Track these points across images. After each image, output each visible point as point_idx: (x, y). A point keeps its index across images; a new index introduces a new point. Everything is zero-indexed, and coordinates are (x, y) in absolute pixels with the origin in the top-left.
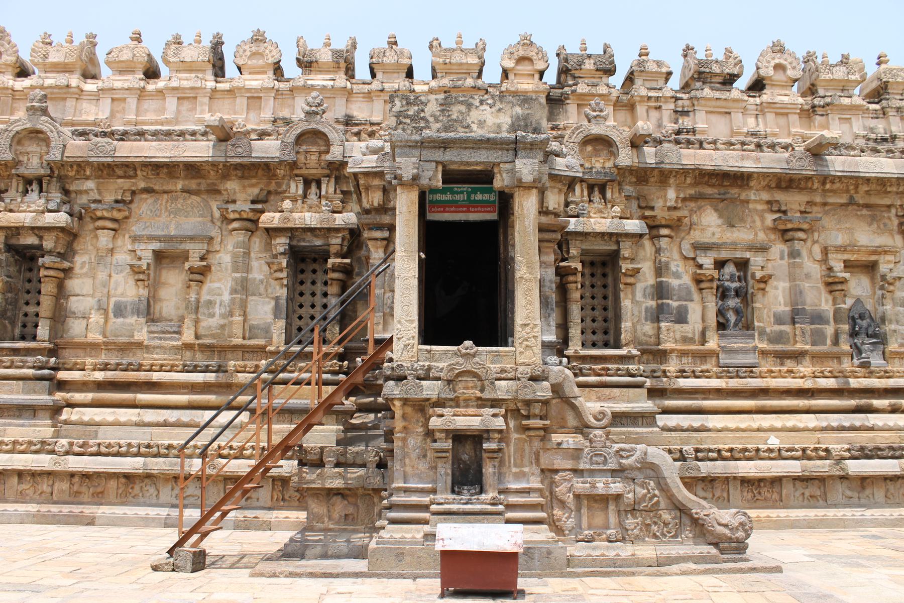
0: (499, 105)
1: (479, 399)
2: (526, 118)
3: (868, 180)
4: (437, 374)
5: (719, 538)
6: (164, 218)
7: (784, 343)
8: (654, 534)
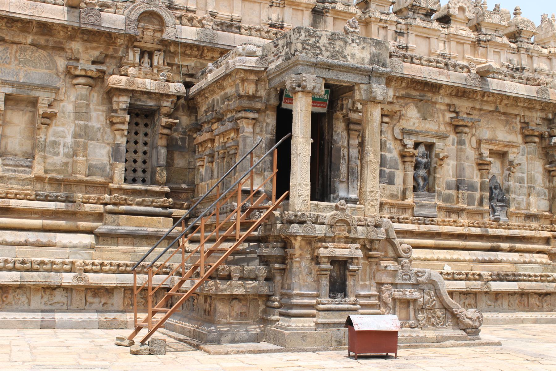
0: (362, 45)
1: (346, 237)
2: (378, 55)
3: (508, 97)
4: (322, 221)
5: (466, 326)
6: (13, 66)
7: (451, 202)
8: (433, 324)
